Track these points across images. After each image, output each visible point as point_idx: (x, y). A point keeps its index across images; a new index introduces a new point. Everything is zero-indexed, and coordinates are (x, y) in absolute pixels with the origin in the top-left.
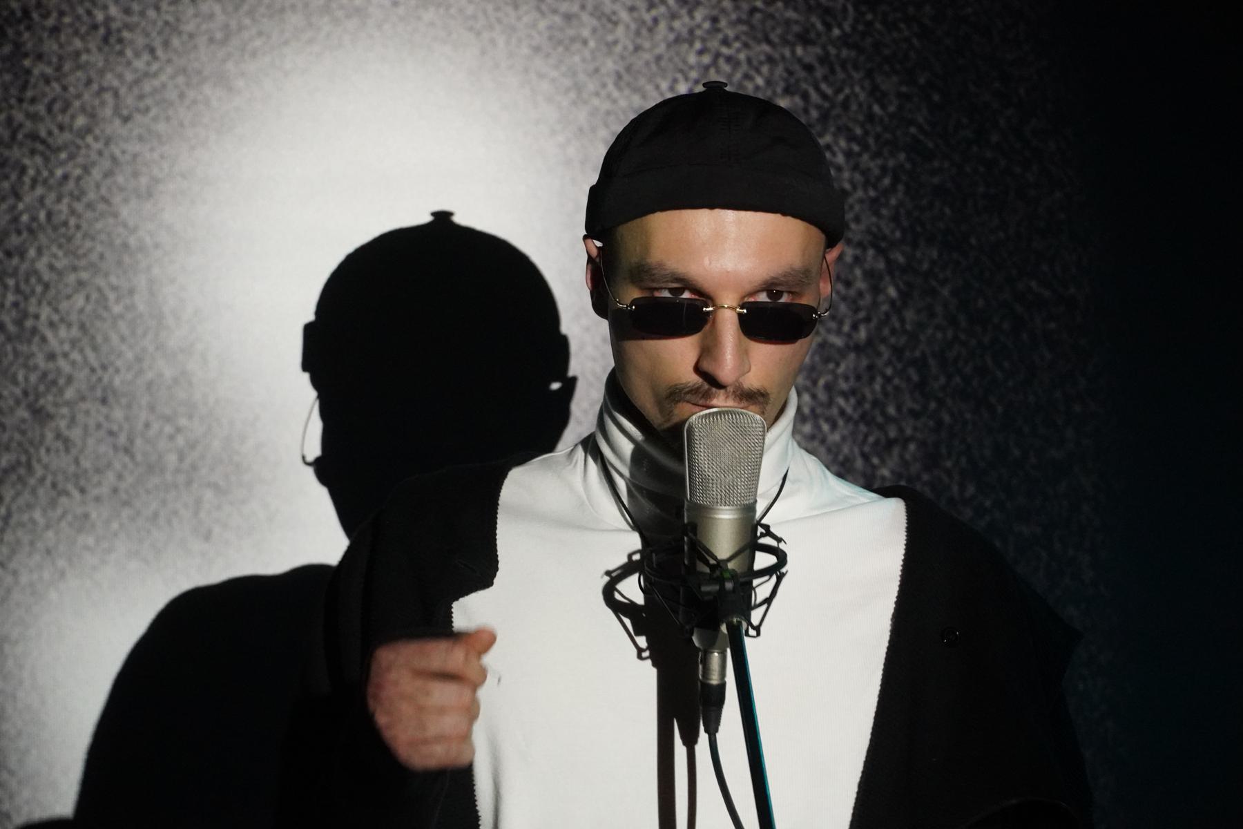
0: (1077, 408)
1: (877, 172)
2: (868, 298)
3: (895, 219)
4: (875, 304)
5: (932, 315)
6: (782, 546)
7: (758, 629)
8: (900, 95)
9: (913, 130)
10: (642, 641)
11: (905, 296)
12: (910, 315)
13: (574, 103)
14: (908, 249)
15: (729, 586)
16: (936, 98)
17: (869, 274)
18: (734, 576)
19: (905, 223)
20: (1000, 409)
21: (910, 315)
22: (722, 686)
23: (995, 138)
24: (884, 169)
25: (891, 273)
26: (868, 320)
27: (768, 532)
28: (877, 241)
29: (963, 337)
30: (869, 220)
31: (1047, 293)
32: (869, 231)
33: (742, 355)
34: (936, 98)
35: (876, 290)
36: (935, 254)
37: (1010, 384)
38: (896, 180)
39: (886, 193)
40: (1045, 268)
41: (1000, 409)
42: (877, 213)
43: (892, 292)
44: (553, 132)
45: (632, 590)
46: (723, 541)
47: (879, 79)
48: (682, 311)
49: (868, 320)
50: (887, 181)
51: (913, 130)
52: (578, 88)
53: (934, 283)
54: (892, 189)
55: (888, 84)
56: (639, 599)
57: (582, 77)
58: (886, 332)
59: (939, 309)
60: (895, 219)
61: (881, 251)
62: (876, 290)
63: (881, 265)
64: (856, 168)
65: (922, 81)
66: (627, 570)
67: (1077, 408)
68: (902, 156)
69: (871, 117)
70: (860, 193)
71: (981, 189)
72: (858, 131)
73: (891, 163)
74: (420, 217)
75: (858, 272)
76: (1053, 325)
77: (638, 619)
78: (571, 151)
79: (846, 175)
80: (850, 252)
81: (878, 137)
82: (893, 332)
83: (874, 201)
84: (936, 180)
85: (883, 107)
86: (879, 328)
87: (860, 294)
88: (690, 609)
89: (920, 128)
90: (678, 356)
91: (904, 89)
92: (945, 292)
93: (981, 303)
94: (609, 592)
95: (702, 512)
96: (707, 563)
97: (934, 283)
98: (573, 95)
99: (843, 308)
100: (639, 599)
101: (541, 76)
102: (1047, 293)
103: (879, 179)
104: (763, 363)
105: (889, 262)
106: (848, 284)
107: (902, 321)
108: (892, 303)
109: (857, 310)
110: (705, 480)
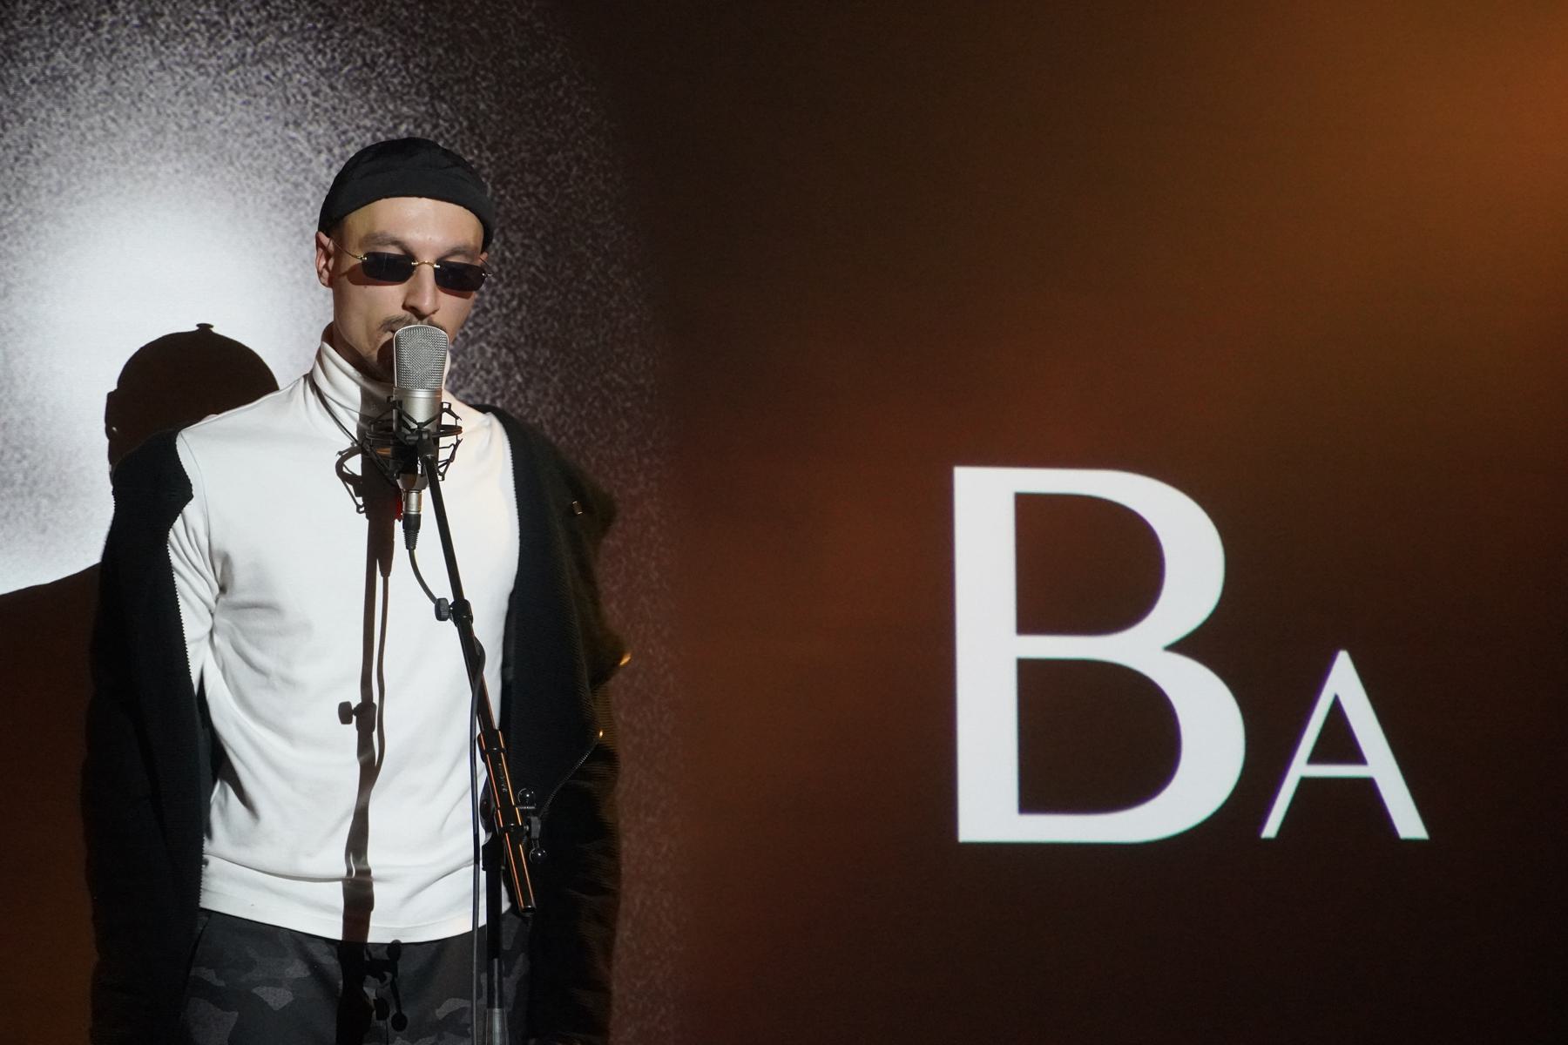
0: (646, 461)
1: (508, 297)
2: (502, 382)
3: (520, 328)
4: (507, 384)
5: (546, 394)
6: (459, 423)
7: (443, 475)
8: (523, 245)
9: (532, 269)
10: (360, 500)
11: (527, 381)
12: (530, 394)
13: (300, 243)
14: (529, 349)
15: (425, 436)
16: (548, 248)
17: (503, 366)
18: (428, 431)
19: (528, 332)
20: (593, 460)
21: (530, 394)
22: (418, 517)
23: (588, 277)
24: (513, 295)
25: (517, 365)
26: (502, 396)
27: (449, 411)
28: (508, 344)
29: (568, 410)
30: (502, 329)
31: (625, 383)
32: (502, 336)
33: (436, 297)
34: (548, 248)
35: (507, 376)
36: (548, 354)
37: (601, 443)
38: (521, 303)
39: (514, 310)
40: (623, 365)
41: (593, 460)
42: (508, 325)
43: (519, 378)
44: (286, 263)
45: (355, 465)
46: (420, 410)
47: (509, 234)
48: (393, 266)
49: (502, 396)
50: (515, 303)
51: (532, 269)
52: (303, 232)
53: (547, 373)
54: (519, 307)
55: (515, 237)
56: (359, 473)
57: (306, 226)
58: (515, 405)
59: (551, 391)
60: (520, 328)
61: (510, 350)
62: (507, 376)
63: (511, 360)
64: (493, 293)
65: (538, 236)
66: (350, 453)
67: (646, 461)
68: (525, 287)
69: (504, 260)
70: (496, 311)
71: (579, 311)
72: (495, 269)
73: (518, 291)
74: (190, 327)
75: (495, 364)
76: (629, 404)
77: (358, 485)
78: (298, 276)
79: (487, 298)
80: (489, 351)
81: (508, 273)
82: (520, 405)
83: (506, 316)
84: (548, 303)
85: (512, 253)
86: (509, 402)
87: (497, 378)
88: (392, 471)
89: (537, 268)
90: (390, 297)
91: (526, 241)
92: (555, 379)
93: (580, 387)
94: (339, 466)
95: (406, 394)
96: (408, 427)
97: (547, 373)
98: (299, 237)
99: (485, 387)
100: (359, 473)
101: (277, 224)
102: (625, 383)
103: (509, 301)
104: (448, 308)
105: (516, 358)
106: (489, 372)
107: (526, 398)
108: (519, 385)
109: (495, 390)
110: (408, 372)
